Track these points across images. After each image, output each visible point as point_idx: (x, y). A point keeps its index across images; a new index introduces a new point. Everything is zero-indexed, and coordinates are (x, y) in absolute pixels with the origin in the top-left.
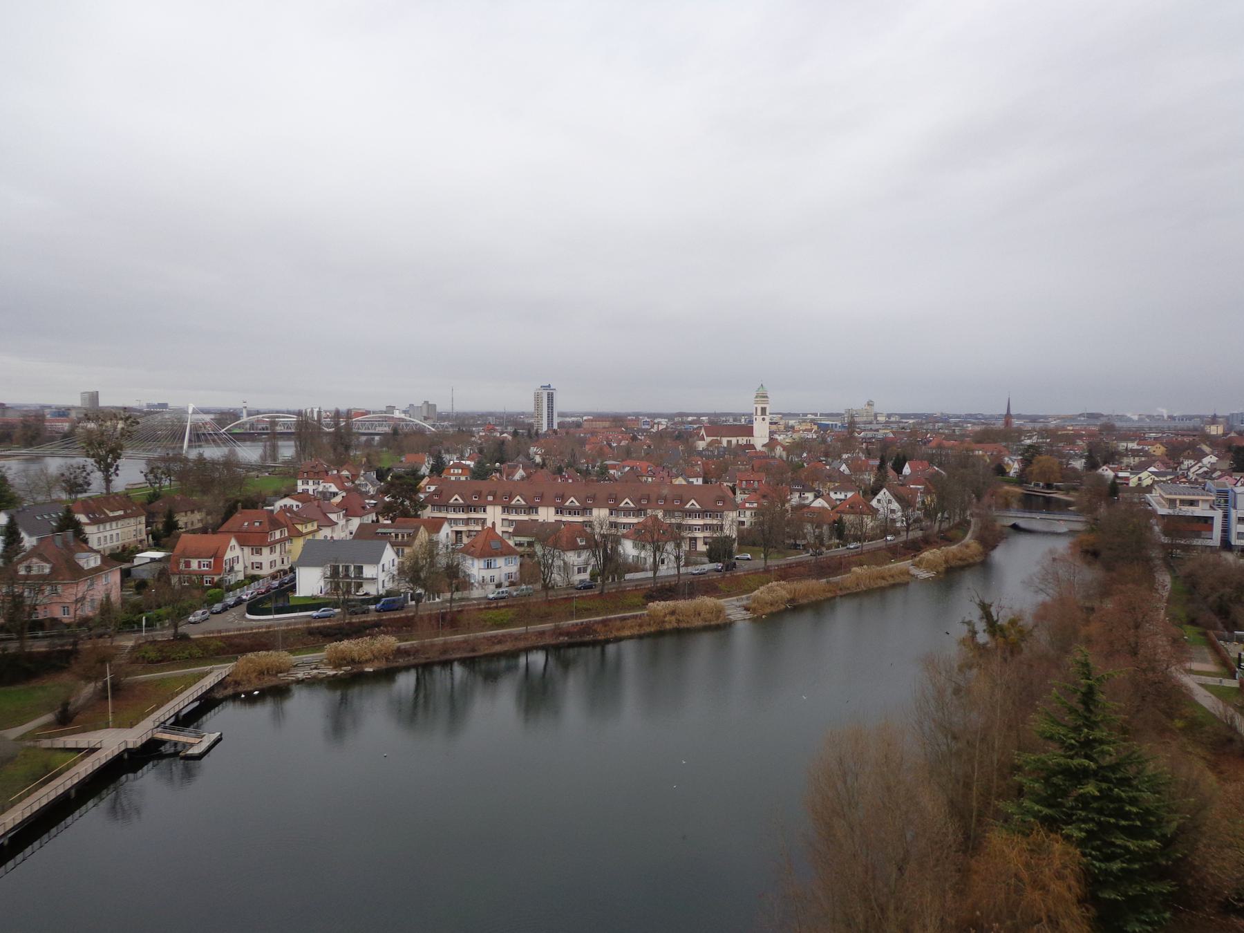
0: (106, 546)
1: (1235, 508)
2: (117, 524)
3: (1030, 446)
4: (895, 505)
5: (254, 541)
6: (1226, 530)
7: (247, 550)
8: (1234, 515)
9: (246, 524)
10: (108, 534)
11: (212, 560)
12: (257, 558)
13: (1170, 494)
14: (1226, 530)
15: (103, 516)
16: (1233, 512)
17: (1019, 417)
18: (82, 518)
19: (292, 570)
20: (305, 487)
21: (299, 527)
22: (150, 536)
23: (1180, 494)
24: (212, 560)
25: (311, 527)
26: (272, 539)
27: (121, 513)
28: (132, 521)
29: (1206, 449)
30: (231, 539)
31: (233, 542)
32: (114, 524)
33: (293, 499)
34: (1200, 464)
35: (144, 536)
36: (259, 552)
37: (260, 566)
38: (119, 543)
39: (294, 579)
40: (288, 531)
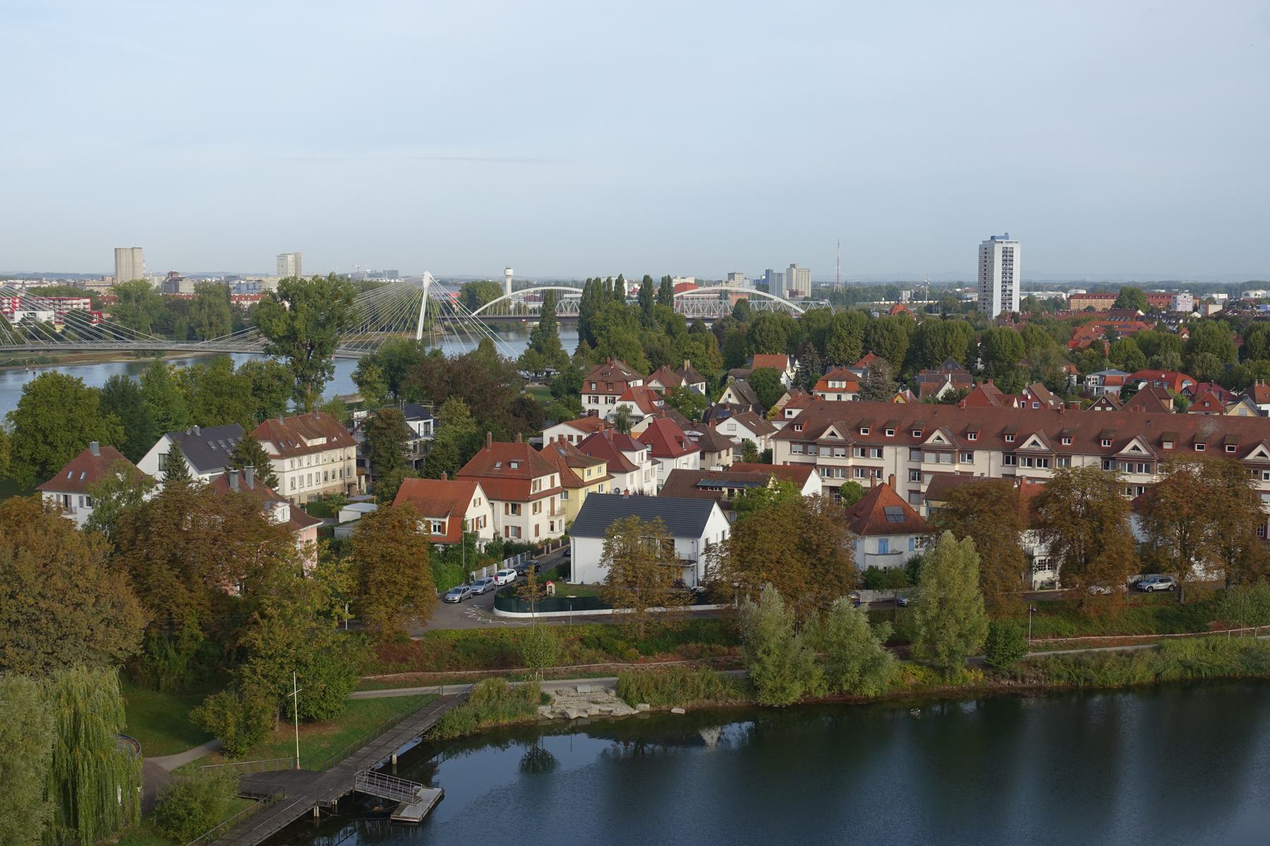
0: (302, 491)
2: (317, 461)
7: (500, 506)
9: (498, 465)
10: (305, 473)
12: (513, 520)
15: (298, 446)
18: (268, 447)
19: (565, 540)
21: (577, 471)
22: (363, 478)
25: (599, 471)
26: (537, 491)
27: (322, 441)
28: (337, 453)
31: (478, 493)
32: (313, 456)
35: (355, 478)
36: (516, 509)
37: (518, 531)
38: (321, 486)
39: (567, 554)
40: (562, 479)
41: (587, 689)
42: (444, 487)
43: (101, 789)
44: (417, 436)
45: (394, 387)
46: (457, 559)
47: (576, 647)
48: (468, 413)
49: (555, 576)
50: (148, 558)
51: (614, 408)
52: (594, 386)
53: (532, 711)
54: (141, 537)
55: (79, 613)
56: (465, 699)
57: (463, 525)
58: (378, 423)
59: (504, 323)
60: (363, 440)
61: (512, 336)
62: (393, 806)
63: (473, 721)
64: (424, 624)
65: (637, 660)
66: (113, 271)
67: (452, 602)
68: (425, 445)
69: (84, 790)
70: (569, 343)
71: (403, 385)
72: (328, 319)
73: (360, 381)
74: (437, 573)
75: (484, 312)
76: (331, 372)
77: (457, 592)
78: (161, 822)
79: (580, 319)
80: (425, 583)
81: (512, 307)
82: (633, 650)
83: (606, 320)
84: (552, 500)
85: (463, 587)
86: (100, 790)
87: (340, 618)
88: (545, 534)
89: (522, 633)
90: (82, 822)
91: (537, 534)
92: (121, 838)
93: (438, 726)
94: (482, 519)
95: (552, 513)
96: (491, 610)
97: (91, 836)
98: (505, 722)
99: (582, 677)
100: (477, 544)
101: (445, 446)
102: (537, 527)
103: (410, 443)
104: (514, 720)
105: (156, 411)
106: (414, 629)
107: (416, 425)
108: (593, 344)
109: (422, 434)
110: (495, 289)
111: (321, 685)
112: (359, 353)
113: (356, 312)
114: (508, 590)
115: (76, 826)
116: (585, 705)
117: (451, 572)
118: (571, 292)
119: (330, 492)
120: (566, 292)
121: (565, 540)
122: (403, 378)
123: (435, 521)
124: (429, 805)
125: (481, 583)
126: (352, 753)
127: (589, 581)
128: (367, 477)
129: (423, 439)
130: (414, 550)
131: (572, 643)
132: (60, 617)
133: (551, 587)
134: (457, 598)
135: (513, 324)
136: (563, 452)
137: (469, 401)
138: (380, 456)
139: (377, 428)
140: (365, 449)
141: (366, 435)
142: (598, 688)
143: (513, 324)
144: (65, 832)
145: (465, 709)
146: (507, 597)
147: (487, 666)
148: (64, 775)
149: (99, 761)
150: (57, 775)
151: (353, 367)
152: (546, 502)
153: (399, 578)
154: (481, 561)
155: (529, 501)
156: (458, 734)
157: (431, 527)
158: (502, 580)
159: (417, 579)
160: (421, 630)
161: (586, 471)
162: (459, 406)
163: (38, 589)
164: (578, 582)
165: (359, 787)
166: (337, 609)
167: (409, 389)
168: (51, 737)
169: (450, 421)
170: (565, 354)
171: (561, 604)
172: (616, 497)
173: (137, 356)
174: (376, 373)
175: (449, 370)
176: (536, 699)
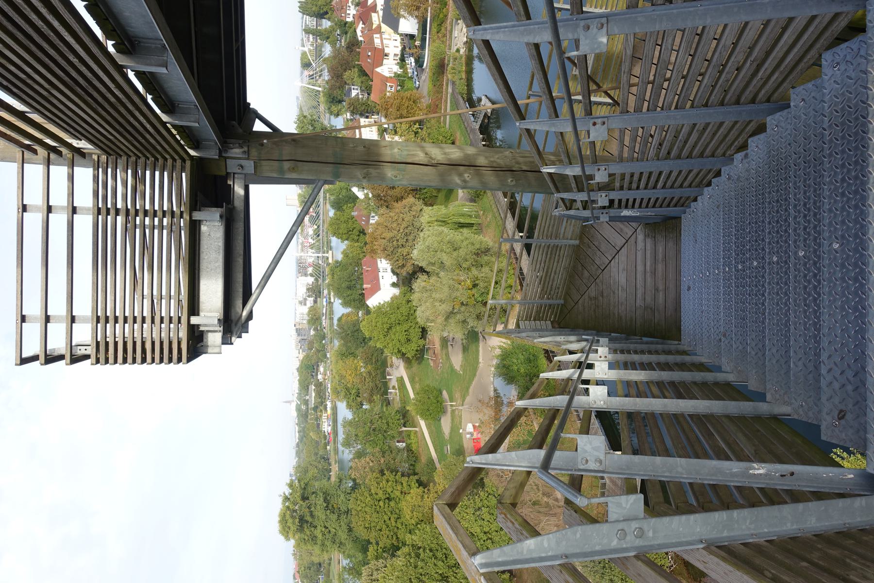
5: (381, 55)
11: (388, 84)
19: (401, 35)
20: (351, 16)
21: (374, 26)
22: (373, 117)
24: (388, 84)
25: (374, 16)
26: (380, 45)
30: (376, 71)
33: (358, 26)
35: (372, 120)
37: (395, 55)
39: (407, 35)
40: (377, 33)
41: (456, 32)
42: (376, 84)
43: (463, 215)
44: (358, 93)
45: (340, 102)
46: (404, 81)
47: (440, 35)
48: (350, 71)
49: (413, 41)
50: (391, 197)
51: (352, 7)
52: (343, 15)
53: (461, 57)
54: (383, 198)
55: (405, 219)
56: (454, 83)
57: (391, 78)
58: (351, 109)
59: (318, 51)
60: (358, 115)
61: (323, 50)
62: (486, 115)
63: (462, 81)
64: (424, 97)
65: (448, 10)
66: (295, 207)
67: (419, 85)
68: (362, 91)
69: (462, 220)
70: (326, 24)
71: (339, 97)
72: (312, 126)
73: (337, 115)
74: (408, 90)
75: (313, 61)
76: (333, 126)
77: (415, 82)
78: (478, 197)
79: (316, 17)
80: (409, 95)
81: (312, 48)
82: (444, 10)
83: (316, 6)
84: (385, 39)
85: (414, 80)
86: (463, 215)
87: (417, 128)
88: (398, 43)
89: (433, 57)
90: (472, 222)
91: (398, 47)
92: (481, 210)
93: (462, 94)
94: (389, 70)
95: (390, 39)
96: (423, 70)
97: (477, 220)
98: (464, 68)
99: (452, 34)
100: (399, 73)
101: (362, 82)
102: (395, 47)
103: (360, 96)
104: (464, 65)
105: (344, 192)
106: (425, 102)
107: (354, 93)
108: (326, 13)
109: (357, 91)
110: (304, 54)
111: (441, 138)
112: (327, 115)
113: (309, 114)
114: (417, 61)
115: (473, 224)
116: (462, 34)
117: (408, 84)
118: (306, 21)
119: (377, 130)
120: (306, 23)
121: (401, 35)
122: (337, 98)
123: (389, 89)
124: (487, 100)
125: (413, 72)
126: (466, 128)
127: (417, 26)
128: (373, 115)
129: (359, 91)
130: (396, 97)
131: (438, 37)
132: (406, 226)
133: (418, 43)
134: (417, 83)
135: (318, 49)
136: (366, 32)
137: (345, 70)
138: (364, 109)
139: (353, 109)
140: (362, 115)
141: (356, 114)
142: (456, 27)
143: (318, 49)
144: (475, 228)
145: (457, 83)
146: (419, 62)
147: (443, 73)
148: (456, 226)
149: (453, 215)
150: (456, 229)
151: (332, 117)
152: (385, 42)
153: (406, 105)
154: (405, 72)
155: (384, 49)
156: (466, 88)
157: (391, 89)
158: (413, 64)
159: (407, 98)
160: (427, 98)
161: (374, 23)
162: (347, 75)
163: (396, 232)
164: (417, 31)
165: (478, 127)
166: (414, 129)
167: (341, 96)
168: (445, 230)
169: (353, 79)
170: (330, 27)
171: (423, 40)
172: (384, 10)
173: (326, 200)
174: (334, 108)
175: (333, 78)
176: (457, 54)
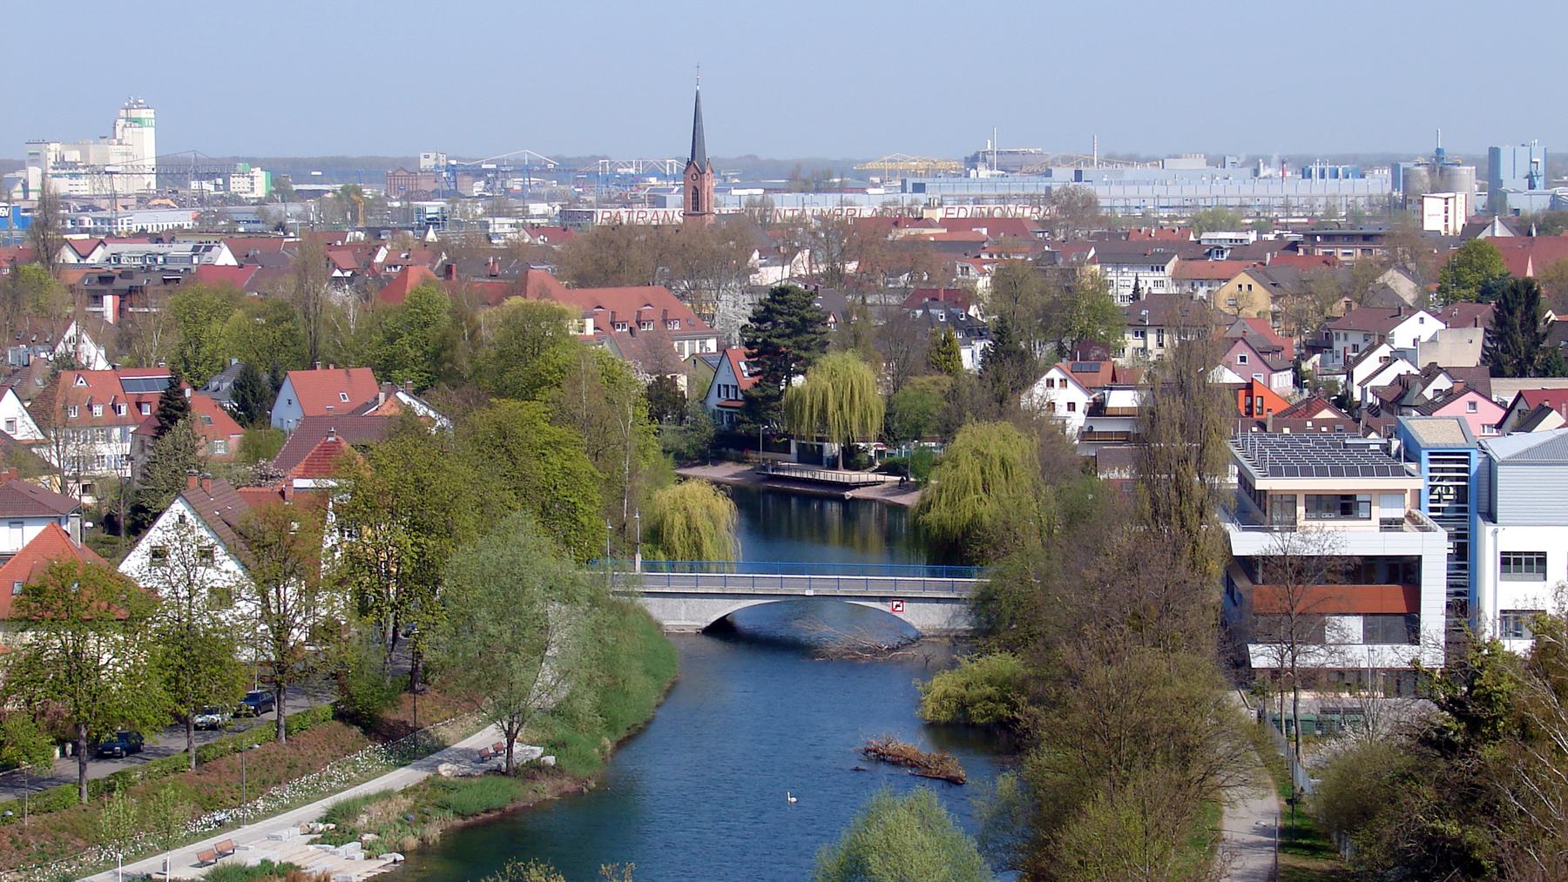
1: (1491, 517)
3: (780, 294)
4: (226, 570)
6: (1462, 604)
8: (1493, 541)
13: (1275, 472)
14: (1462, 604)
16: (1486, 530)
17: (751, 172)
23: (1307, 472)
29: (1405, 288)
34: (1384, 350)
